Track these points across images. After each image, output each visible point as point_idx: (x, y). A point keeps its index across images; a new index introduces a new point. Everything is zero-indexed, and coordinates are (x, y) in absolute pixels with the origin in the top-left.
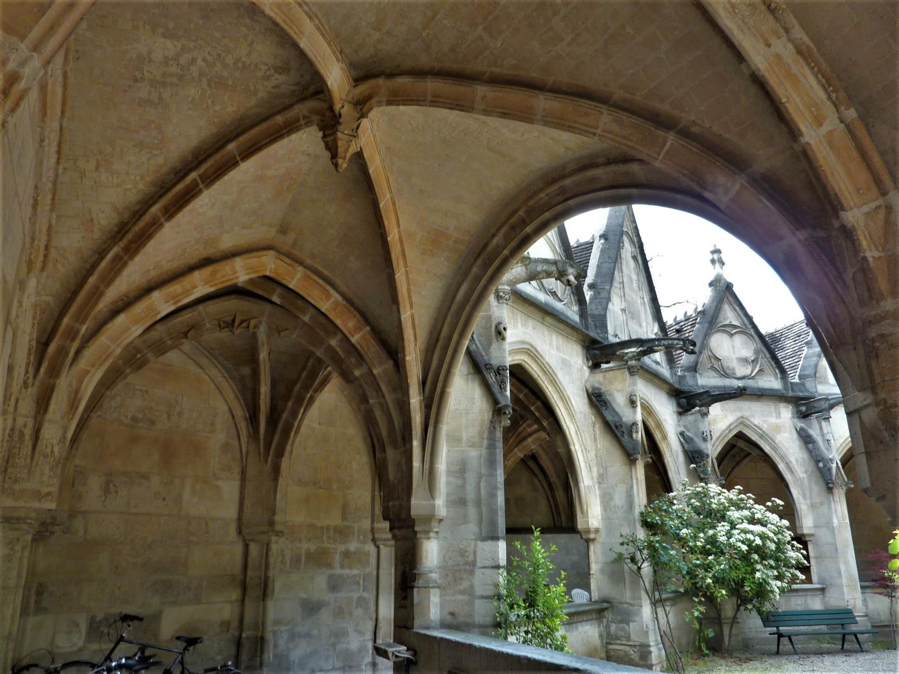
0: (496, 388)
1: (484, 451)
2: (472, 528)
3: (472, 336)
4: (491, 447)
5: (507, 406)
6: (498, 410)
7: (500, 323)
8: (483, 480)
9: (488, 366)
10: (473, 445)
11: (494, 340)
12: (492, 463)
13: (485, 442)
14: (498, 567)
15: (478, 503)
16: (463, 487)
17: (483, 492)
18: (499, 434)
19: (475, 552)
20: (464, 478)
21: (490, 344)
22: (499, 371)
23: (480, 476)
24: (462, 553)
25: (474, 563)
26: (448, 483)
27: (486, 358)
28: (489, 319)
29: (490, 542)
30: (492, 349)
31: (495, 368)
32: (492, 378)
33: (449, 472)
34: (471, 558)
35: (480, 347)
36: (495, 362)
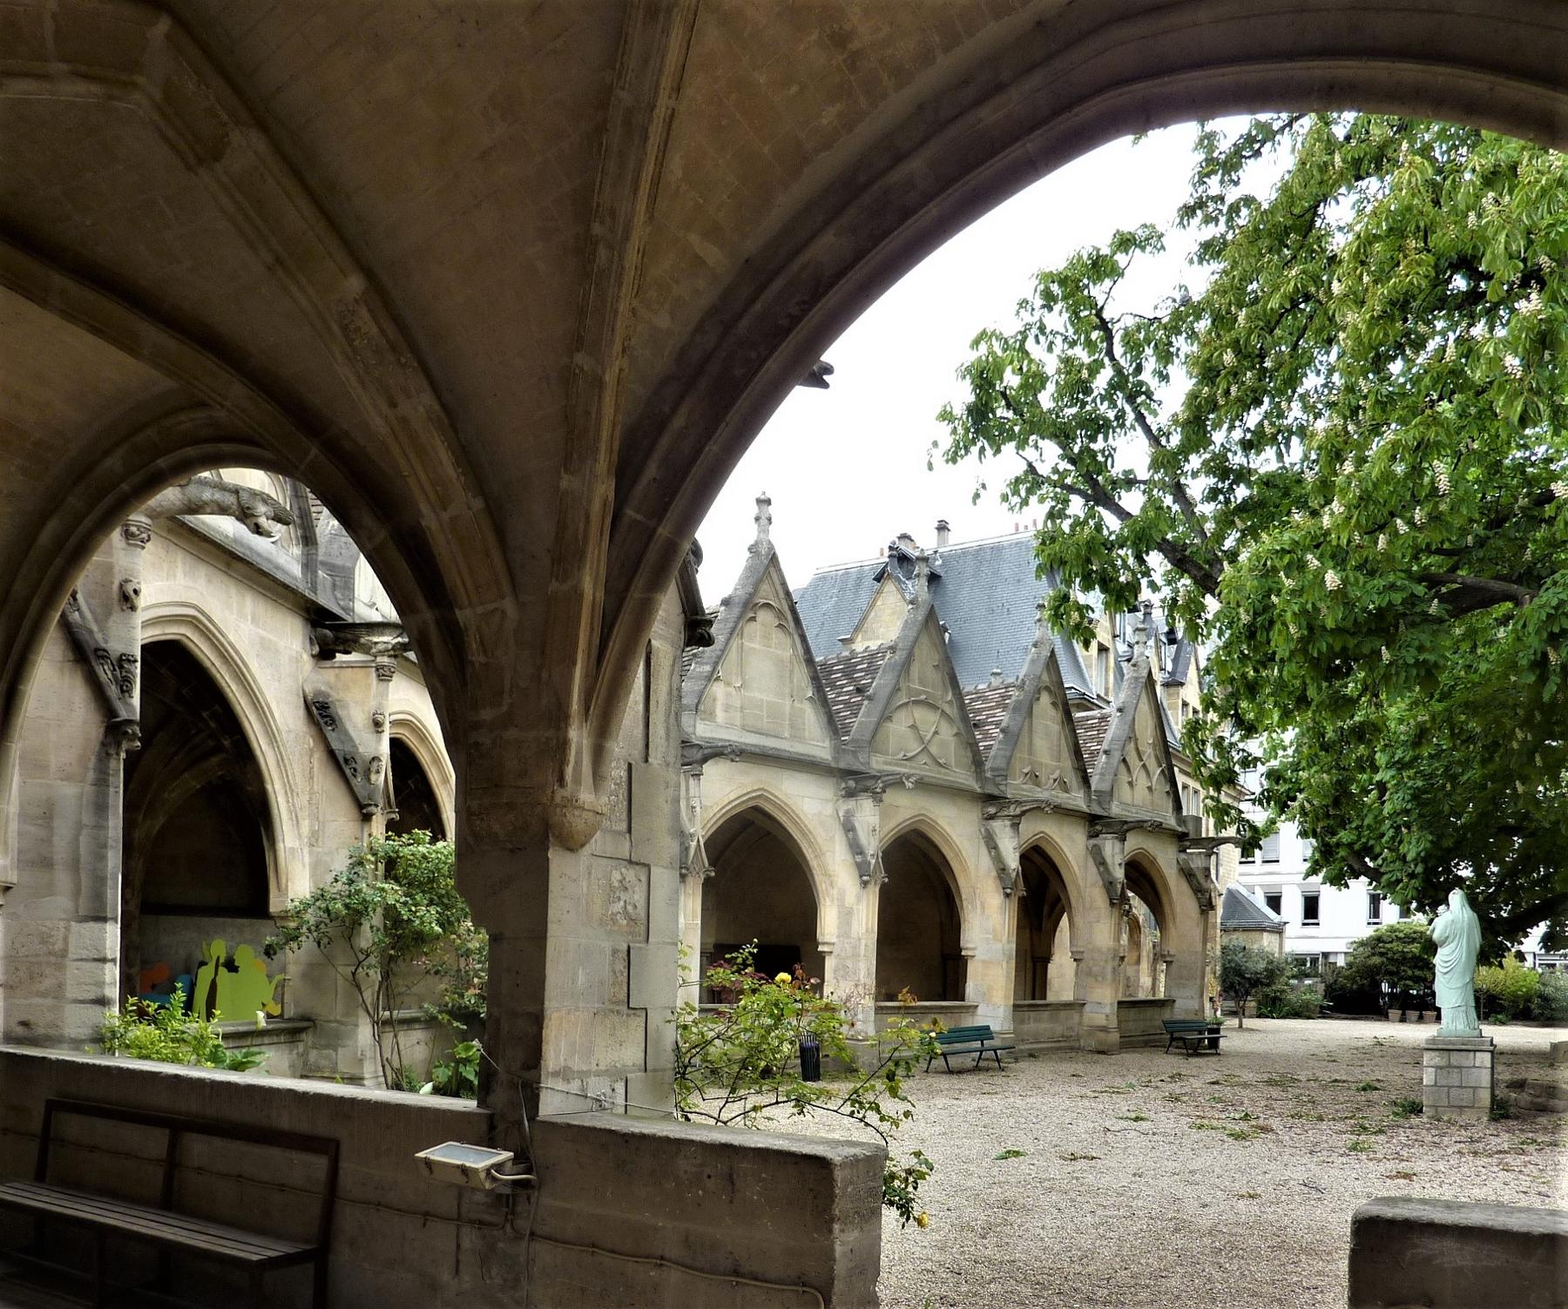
0: (113, 691)
1: (89, 789)
2: (62, 902)
3: (74, 596)
4: (102, 781)
5: (130, 722)
6: (114, 729)
7: (127, 581)
8: (85, 832)
9: (102, 654)
10: (68, 778)
11: (116, 608)
12: (101, 808)
13: (91, 775)
14: (104, 960)
15: (75, 866)
16: (48, 841)
17: (83, 851)
18: (118, 767)
19: (66, 939)
20: (50, 829)
21: (108, 614)
22: (124, 661)
23: (79, 826)
24: (44, 939)
25: (64, 953)
26: (20, 834)
27: (99, 636)
28: (109, 569)
29: (91, 924)
30: (110, 623)
31: (114, 655)
32: (104, 673)
33: (23, 816)
34: (59, 946)
35: (88, 615)
36: (115, 647)
